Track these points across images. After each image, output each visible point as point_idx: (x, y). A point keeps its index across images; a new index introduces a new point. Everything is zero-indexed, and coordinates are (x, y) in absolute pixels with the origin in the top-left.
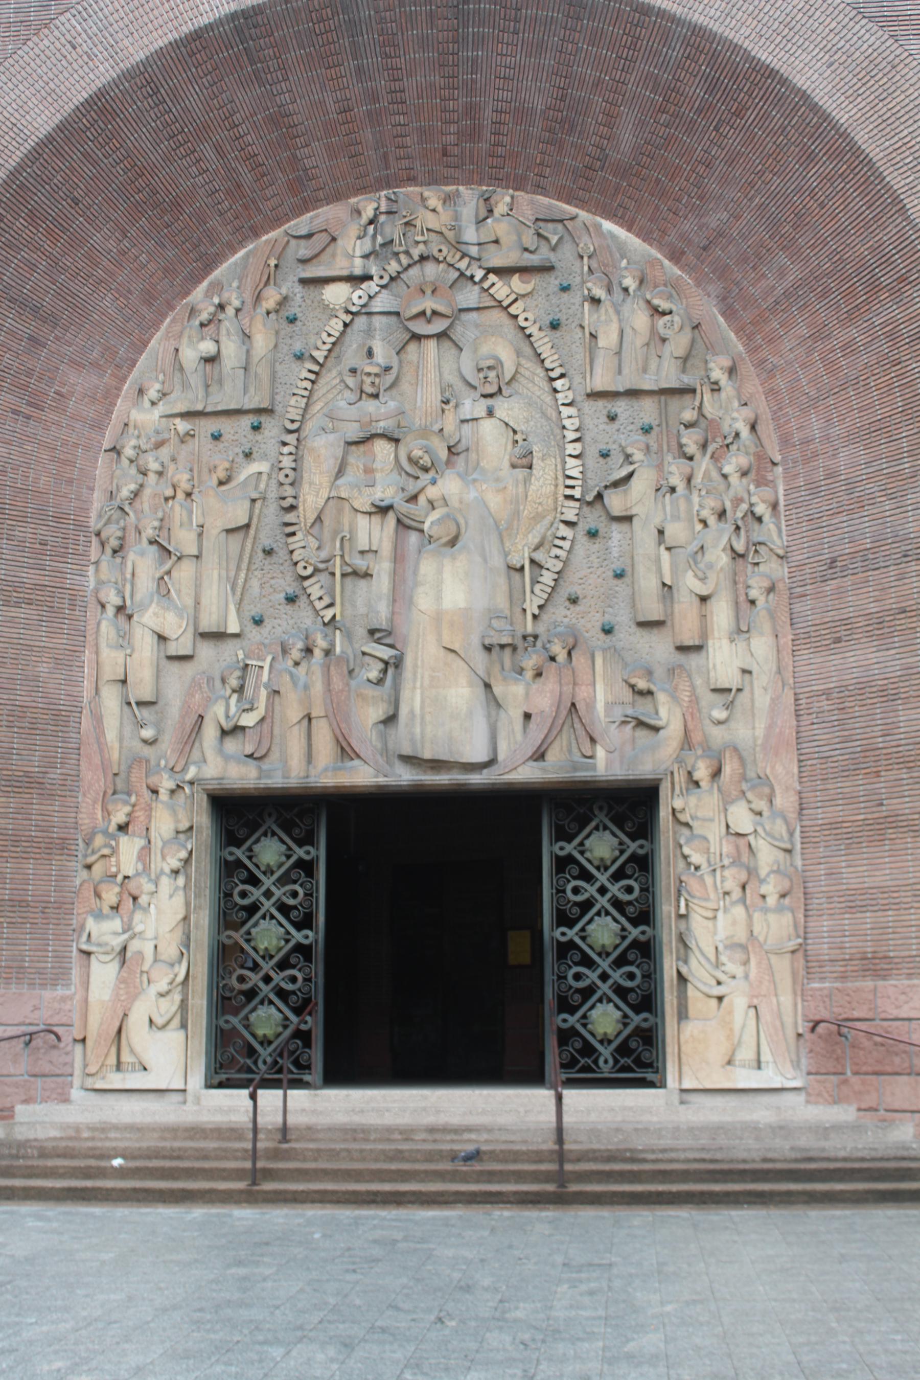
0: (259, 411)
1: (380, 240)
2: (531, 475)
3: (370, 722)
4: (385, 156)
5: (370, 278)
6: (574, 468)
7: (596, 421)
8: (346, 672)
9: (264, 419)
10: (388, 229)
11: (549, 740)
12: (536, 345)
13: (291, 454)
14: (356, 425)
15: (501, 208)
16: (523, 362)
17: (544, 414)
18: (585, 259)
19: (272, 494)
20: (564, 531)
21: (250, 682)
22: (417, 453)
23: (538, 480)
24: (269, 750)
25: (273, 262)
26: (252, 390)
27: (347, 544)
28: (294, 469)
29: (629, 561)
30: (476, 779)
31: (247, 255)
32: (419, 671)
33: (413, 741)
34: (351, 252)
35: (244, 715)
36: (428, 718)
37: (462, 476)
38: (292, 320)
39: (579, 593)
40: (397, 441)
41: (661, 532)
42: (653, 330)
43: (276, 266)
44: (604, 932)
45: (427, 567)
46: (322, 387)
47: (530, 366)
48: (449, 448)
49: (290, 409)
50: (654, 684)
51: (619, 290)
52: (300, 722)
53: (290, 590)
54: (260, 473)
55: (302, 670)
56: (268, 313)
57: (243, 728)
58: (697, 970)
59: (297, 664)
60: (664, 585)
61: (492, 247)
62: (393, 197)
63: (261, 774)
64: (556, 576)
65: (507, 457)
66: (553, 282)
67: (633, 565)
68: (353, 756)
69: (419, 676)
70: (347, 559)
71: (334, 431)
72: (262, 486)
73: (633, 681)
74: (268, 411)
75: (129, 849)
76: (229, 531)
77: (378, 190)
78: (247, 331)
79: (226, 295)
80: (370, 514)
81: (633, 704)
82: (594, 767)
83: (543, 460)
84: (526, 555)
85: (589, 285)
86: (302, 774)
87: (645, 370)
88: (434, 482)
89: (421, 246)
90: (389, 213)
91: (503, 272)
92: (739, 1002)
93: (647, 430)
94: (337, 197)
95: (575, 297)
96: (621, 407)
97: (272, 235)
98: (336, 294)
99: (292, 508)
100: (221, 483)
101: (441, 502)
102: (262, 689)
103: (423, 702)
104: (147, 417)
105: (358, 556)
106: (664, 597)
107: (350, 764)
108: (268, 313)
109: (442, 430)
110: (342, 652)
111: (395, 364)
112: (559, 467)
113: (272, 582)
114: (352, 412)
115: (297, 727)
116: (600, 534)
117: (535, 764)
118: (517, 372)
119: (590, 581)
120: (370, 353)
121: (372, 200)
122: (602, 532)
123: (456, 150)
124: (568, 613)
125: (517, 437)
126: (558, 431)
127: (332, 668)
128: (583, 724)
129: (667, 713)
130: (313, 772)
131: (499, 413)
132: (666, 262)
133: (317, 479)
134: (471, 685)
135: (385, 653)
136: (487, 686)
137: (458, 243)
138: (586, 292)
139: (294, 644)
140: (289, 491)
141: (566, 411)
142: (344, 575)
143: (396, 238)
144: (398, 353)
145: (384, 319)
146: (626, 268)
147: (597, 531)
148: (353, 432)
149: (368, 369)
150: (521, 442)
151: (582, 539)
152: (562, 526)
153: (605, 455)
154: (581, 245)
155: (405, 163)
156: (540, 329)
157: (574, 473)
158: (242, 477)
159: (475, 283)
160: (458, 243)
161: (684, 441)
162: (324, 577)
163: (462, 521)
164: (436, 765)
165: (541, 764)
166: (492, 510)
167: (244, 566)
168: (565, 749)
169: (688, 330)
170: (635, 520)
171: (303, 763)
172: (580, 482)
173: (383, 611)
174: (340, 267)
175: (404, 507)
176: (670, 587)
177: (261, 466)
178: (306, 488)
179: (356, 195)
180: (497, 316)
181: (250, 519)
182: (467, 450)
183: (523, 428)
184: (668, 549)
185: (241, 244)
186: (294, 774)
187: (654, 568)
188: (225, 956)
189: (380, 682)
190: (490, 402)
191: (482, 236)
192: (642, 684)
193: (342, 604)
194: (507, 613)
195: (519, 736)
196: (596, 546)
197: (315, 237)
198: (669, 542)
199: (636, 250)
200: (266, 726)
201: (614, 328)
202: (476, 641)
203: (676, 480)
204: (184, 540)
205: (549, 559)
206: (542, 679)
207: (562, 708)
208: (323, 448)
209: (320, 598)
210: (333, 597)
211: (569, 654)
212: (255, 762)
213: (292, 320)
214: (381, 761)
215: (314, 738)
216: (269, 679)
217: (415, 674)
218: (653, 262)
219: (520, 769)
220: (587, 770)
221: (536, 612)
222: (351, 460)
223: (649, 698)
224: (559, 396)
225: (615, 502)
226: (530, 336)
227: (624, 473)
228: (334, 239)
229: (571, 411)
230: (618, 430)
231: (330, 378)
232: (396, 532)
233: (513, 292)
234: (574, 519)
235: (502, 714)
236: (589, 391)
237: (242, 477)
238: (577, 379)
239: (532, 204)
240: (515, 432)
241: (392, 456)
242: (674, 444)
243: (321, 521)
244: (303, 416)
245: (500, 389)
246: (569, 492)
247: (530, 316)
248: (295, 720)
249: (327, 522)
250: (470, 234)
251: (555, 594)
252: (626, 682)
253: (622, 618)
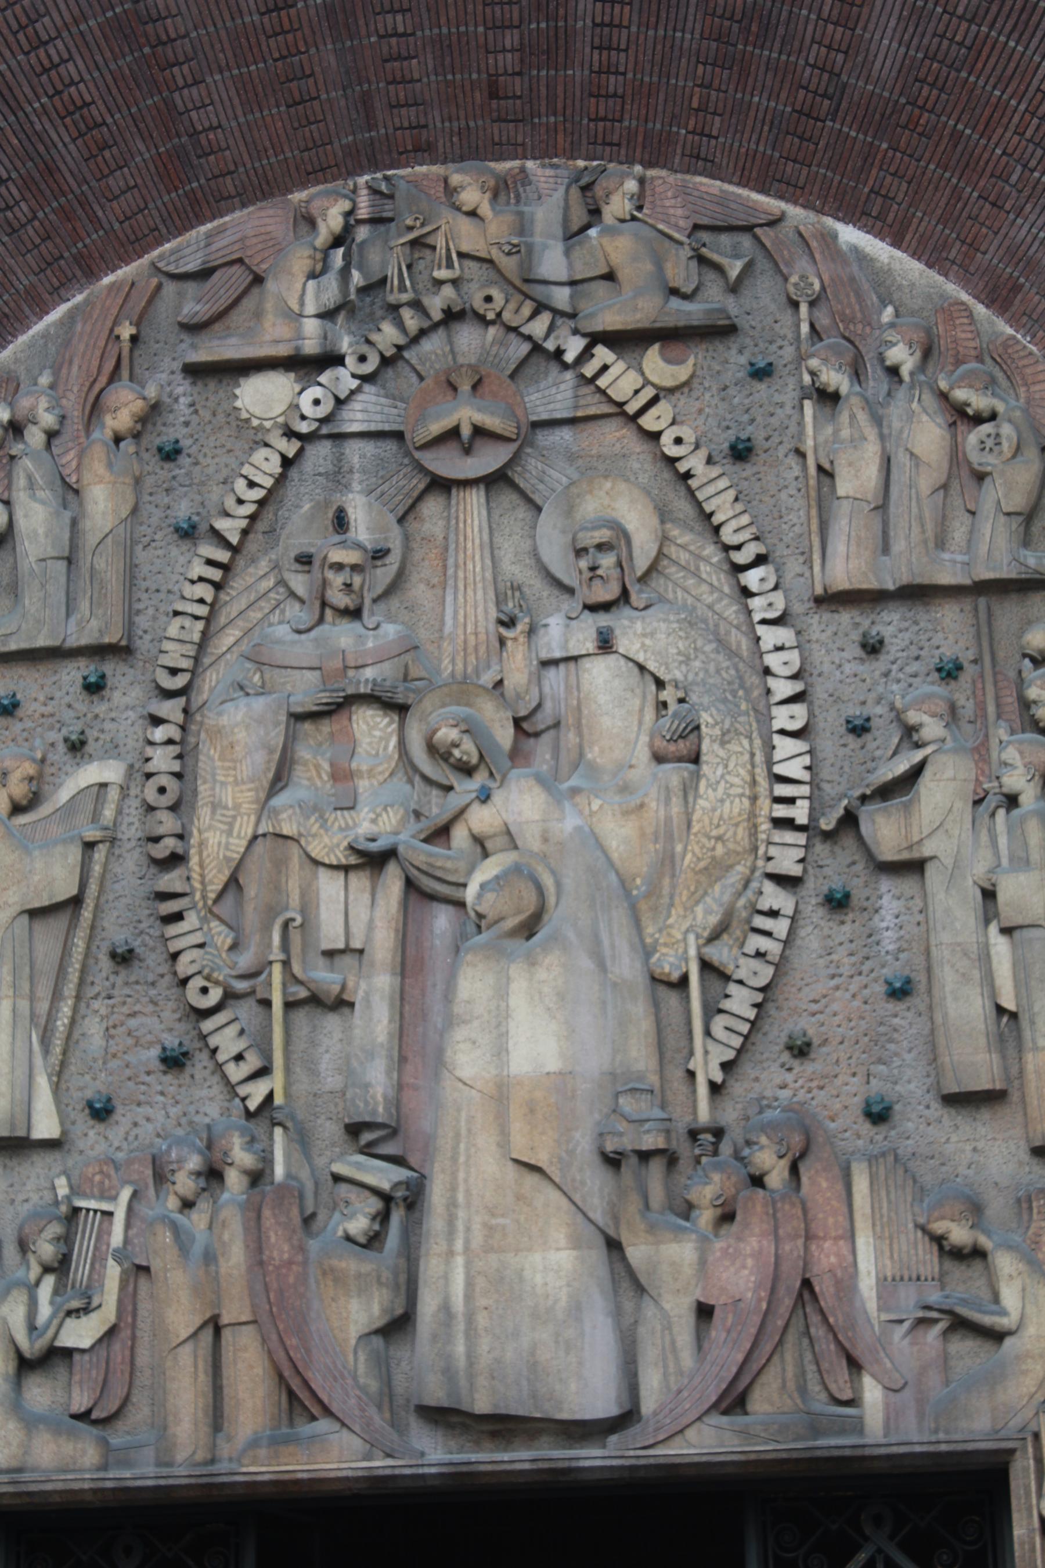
0: (100, 651)
1: (357, 277)
2: (697, 776)
3: (354, 1332)
4: (366, 100)
5: (338, 360)
6: (791, 758)
7: (837, 656)
8: (297, 1220)
9: (109, 667)
10: (374, 257)
11: (755, 1367)
12: (700, 496)
13: (170, 742)
14: (312, 677)
15: (618, 206)
16: (675, 532)
17: (722, 644)
18: (804, 308)
19: (131, 830)
20: (774, 897)
21: (84, 1247)
22: (447, 734)
23: (713, 786)
24: (126, 1400)
25: (126, 331)
26: (84, 606)
27: (295, 937)
28: (178, 776)
29: (920, 961)
30: (592, 1456)
31: (71, 317)
32: (461, 1214)
33: (449, 1373)
34: (297, 304)
35: (70, 1323)
36: (482, 1320)
37: (547, 783)
38: (170, 454)
39: (811, 1032)
40: (402, 709)
41: (989, 895)
42: (956, 456)
43: (134, 339)
45: (474, 984)
46: (237, 598)
47: (687, 539)
48: (517, 722)
49: (168, 646)
50: (988, 1234)
51: (880, 372)
52: (194, 1335)
53: (171, 1041)
54: (104, 785)
55: (198, 1220)
56: (118, 439)
57: (68, 1353)
59: (187, 1205)
60: (1000, 1010)
61: (601, 288)
62: (383, 187)
63: (109, 1456)
64: (759, 997)
65: (644, 739)
66: (735, 359)
67: (929, 970)
68: (315, 1410)
69: (460, 1226)
70: (297, 969)
71: (263, 691)
72: (108, 813)
73: (939, 1227)
74: (121, 651)
76: (34, 914)
77: (351, 173)
78: (73, 479)
79: (25, 403)
80: (346, 869)
81: (941, 1280)
82: (858, 1426)
83: (723, 743)
84: (692, 952)
85: (814, 363)
86: (200, 1456)
87: (941, 543)
88: (484, 797)
89: (448, 291)
90: (375, 221)
91: (626, 341)
93: (949, 672)
94: (263, 189)
95: (784, 391)
96: (891, 623)
97: (125, 272)
98: (264, 396)
99: (175, 860)
100: (17, 809)
101: (501, 841)
102: (111, 1262)
103: (469, 1284)
105: (321, 961)
106: (1001, 1038)
107: (307, 1429)
108: (118, 439)
109: (500, 683)
110: (289, 1175)
111: (396, 544)
112: (759, 758)
113: (133, 1023)
114: (304, 650)
115: (188, 1348)
116: (854, 901)
117: (724, 1420)
118: (660, 554)
119: (835, 1007)
120: (341, 522)
121: (339, 195)
122: (858, 897)
123: (518, 85)
124: (789, 1077)
125: (666, 695)
126: (753, 680)
127: (267, 1213)
128: (831, 1328)
130: (225, 1450)
131: (625, 644)
132: (980, 310)
133: (228, 796)
134: (576, 1243)
135: (383, 1176)
136: (614, 1246)
137: (527, 281)
138: (807, 379)
139: (180, 1161)
140: (167, 823)
141: (770, 636)
142: (289, 1005)
143: (392, 272)
144: (401, 520)
145: (369, 447)
146: (892, 325)
147: (847, 896)
148: (305, 690)
149: (337, 556)
150: (673, 707)
151: (814, 913)
152: (769, 887)
153: (859, 729)
154: (794, 279)
155: (410, 115)
156: (710, 461)
157: (794, 769)
158: (64, 795)
159: (566, 366)
160: (527, 281)
161: (1033, 693)
162: (245, 1011)
163: (548, 882)
164: (503, 1427)
165: (740, 1420)
166: (615, 856)
167: (70, 989)
168: (791, 1385)
169: (1032, 453)
170: (930, 869)
172: (805, 790)
173: (378, 1079)
174: (273, 338)
175: (419, 854)
176: (1014, 1016)
177: (104, 771)
178: (204, 814)
179: (304, 185)
180: (613, 436)
181: (83, 885)
182: (557, 725)
183: (678, 675)
184: (1007, 931)
185: (58, 294)
186: (181, 1456)
187: (976, 974)
189: (373, 1241)
190: (603, 620)
191: (578, 266)
192: (959, 1234)
193: (287, 1070)
194: (654, 1079)
195: (687, 1359)
196: (846, 930)
197: (217, 275)
198: (1009, 915)
199: (912, 285)
200: (118, 1348)
201: (872, 450)
202: (584, 1143)
203: (1016, 780)
205: (742, 961)
206: (735, 1228)
207: (782, 1291)
208: (241, 730)
209: (239, 1058)
210: (267, 1054)
211: (794, 1170)
212: (95, 1431)
213: (170, 454)
214: (379, 1421)
215: (228, 1372)
216: (126, 1241)
217: (451, 1222)
218: (951, 310)
219: (691, 1434)
220: (842, 1432)
221: (718, 1077)
222: (303, 752)
223: (978, 1265)
224: (755, 603)
225: (886, 831)
226: (688, 475)
227: (901, 766)
228: (258, 280)
229: (783, 635)
230: (886, 674)
231: (254, 577)
232: (405, 905)
233: (647, 382)
234: (796, 870)
235: (649, 1310)
236: (819, 590)
237: (64, 795)
238: (793, 566)
239: (682, 194)
240: (660, 684)
241: (393, 741)
242: (1010, 700)
243: (240, 888)
244: (197, 659)
245: (625, 594)
246: (781, 811)
247: (687, 433)
248: (184, 1334)
249: (251, 890)
250: (553, 263)
251: (757, 1038)
252: (924, 1229)
253: (910, 1087)
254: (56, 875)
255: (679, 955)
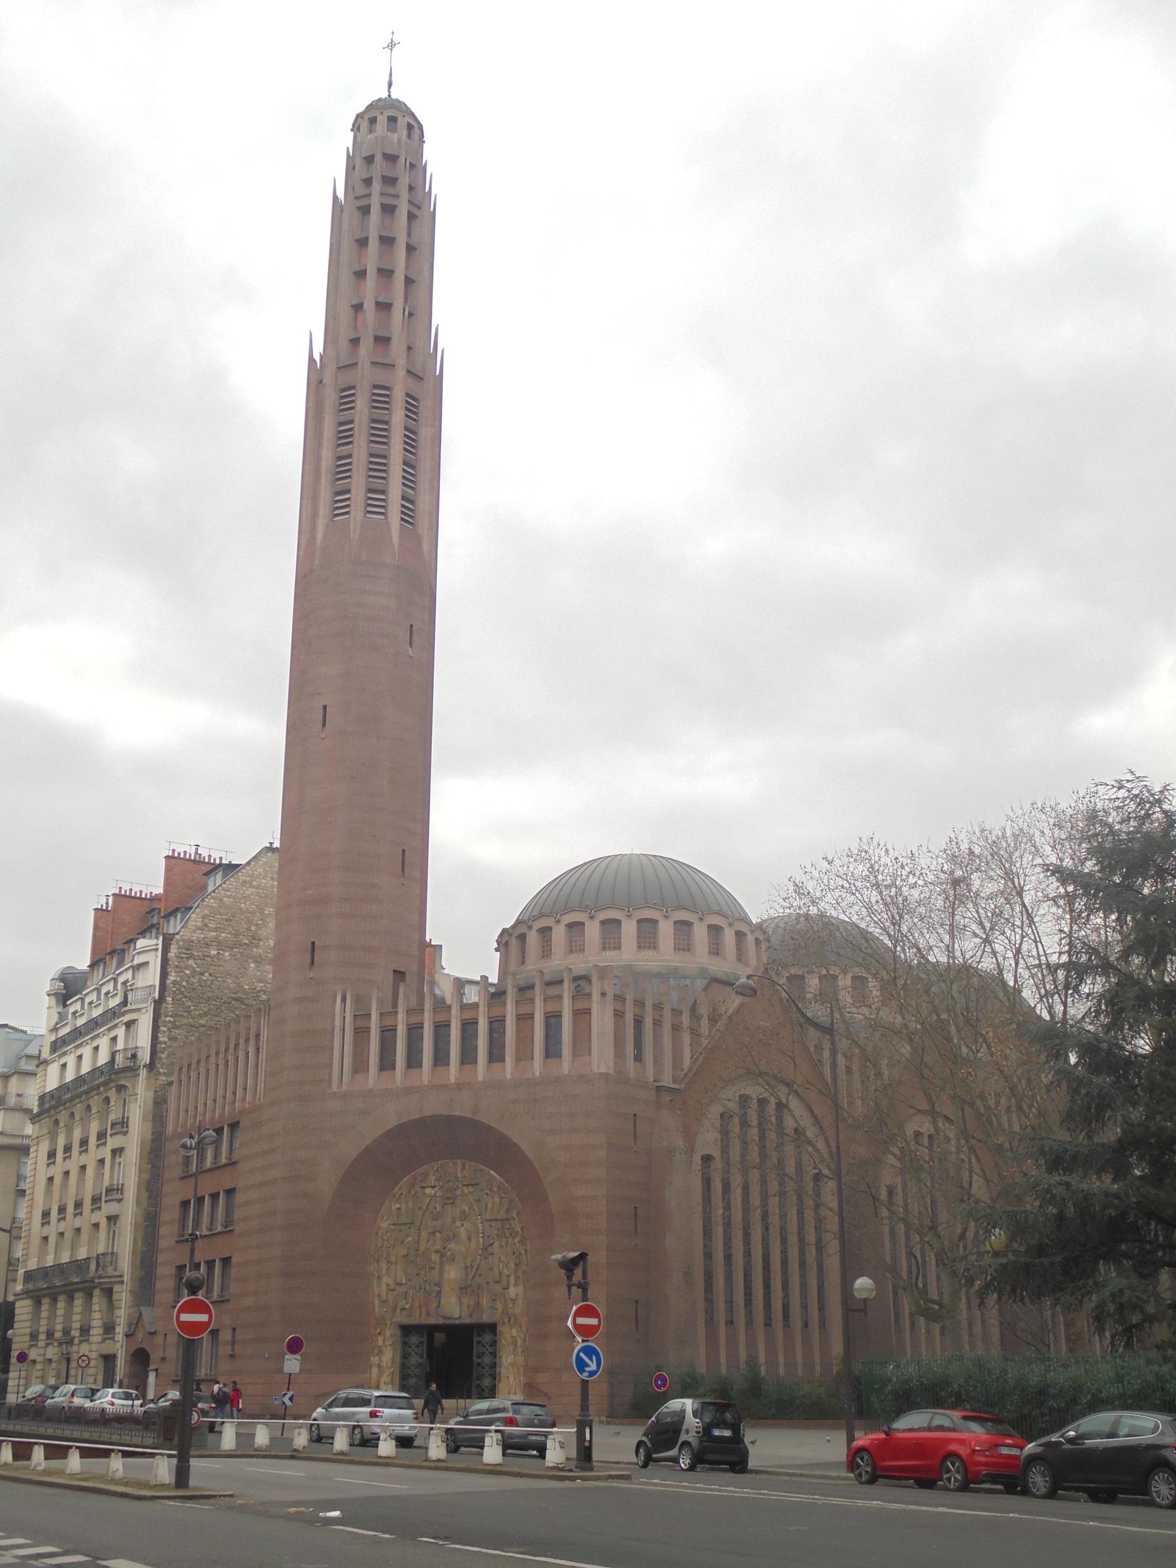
30: (457, 1322)
34: (432, 1179)
44: (487, 1360)
45: (447, 1267)
58: (503, 1370)
75: (380, 1339)
92: (511, 1379)
96: (493, 1223)
104: (384, 1225)
129: (499, 1306)
148: (431, 1230)
171: (419, 1318)
188: (403, 1366)
204: (393, 1259)
208: (424, 1233)
225: (489, 1249)
254: (405, 1252)
255: (468, 1264)
